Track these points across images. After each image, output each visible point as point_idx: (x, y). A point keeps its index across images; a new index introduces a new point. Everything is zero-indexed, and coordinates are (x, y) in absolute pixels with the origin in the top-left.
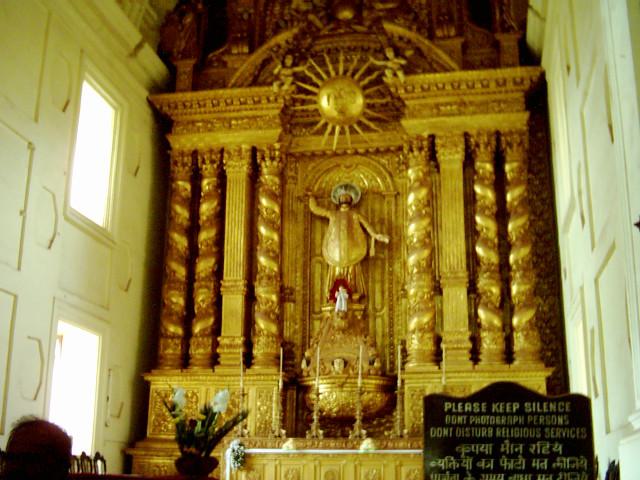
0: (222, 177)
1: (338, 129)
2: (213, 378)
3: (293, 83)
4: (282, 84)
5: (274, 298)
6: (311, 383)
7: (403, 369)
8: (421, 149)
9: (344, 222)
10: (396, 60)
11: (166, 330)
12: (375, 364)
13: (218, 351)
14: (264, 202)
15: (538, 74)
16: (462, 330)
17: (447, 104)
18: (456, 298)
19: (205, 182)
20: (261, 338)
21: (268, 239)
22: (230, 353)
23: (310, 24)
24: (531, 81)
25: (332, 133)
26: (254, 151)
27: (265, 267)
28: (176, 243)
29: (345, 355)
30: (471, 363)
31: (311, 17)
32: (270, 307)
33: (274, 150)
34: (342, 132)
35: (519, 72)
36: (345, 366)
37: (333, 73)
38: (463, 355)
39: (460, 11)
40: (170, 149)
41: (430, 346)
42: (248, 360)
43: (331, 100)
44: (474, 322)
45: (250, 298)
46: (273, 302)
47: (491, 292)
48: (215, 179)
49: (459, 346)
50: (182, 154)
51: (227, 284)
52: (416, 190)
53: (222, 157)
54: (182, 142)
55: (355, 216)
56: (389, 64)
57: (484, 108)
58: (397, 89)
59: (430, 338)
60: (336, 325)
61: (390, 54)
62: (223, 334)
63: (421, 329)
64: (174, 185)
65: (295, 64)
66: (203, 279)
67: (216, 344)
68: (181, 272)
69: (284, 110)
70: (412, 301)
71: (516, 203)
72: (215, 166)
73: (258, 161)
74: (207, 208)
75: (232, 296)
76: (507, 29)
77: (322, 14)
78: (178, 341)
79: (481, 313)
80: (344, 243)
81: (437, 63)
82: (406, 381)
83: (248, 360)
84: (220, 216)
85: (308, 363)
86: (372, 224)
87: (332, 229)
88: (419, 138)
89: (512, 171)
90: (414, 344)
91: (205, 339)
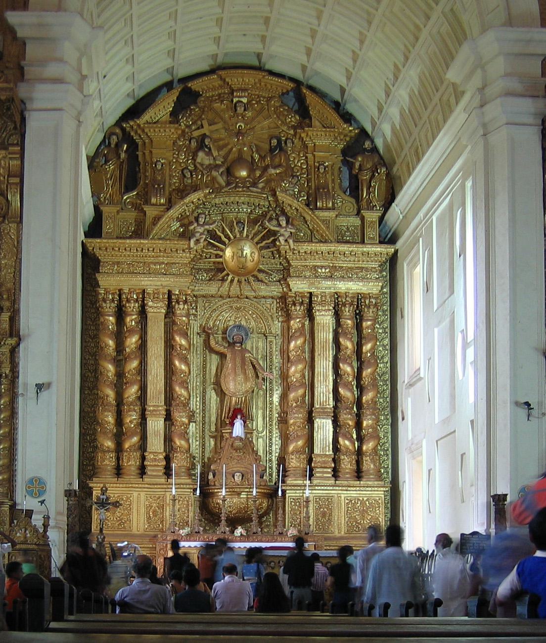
0: (143, 313)
1: (236, 279)
2: (143, 486)
3: (205, 240)
4: (198, 241)
5: (185, 420)
6: (216, 491)
7: (283, 482)
8: (302, 303)
9: (238, 360)
10: (288, 230)
11: (102, 445)
12: (264, 477)
13: (146, 463)
14: (177, 338)
15: (393, 250)
16: (327, 453)
17: (322, 267)
18: (324, 429)
19: (128, 319)
21: (182, 371)
22: (155, 466)
23: (214, 179)
24: (387, 254)
25: (232, 281)
26: (170, 292)
27: (181, 395)
28: (108, 371)
30: (334, 479)
31: (214, 173)
33: (186, 295)
34: (239, 282)
35: (379, 249)
36: (242, 479)
37: (238, 236)
38: (328, 473)
39: (333, 181)
40: (99, 286)
41: (303, 464)
42: (168, 471)
43: (235, 257)
44: (336, 448)
45: (168, 418)
47: (349, 425)
48: (136, 316)
49: (326, 466)
50: (107, 292)
51: (151, 408)
52: (297, 338)
53: (143, 298)
54: (107, 282)
55: (247, 355)
56: (282, 231)
57: (348, 274)
58: (286, 252)
59: (304, 459)
61: (284, 223)
62: (148, 450)
63: (297, 451)
64: (102, 320)
65: (205, 224)
66: (131, 403)
67: (143, 458)
68: (110, 393)
69: (193, 260)
71: (369, 355)
72: (137, 305)
73: (174, 303)
74: (132, 341)
75: (154, 419)
76: (371, 208)
77: (221, 170)
78: (113, 455)
79: (340, 440)
80: (240, 378)
81: (317, 231)
82: (287, 492)
83: (168, 471)
84: (143, 347)
85: (214, 477)
87: (229, 364)
88: (302, 295)
89: (368, 328)
90: (295, 462)
91: (135, 454)
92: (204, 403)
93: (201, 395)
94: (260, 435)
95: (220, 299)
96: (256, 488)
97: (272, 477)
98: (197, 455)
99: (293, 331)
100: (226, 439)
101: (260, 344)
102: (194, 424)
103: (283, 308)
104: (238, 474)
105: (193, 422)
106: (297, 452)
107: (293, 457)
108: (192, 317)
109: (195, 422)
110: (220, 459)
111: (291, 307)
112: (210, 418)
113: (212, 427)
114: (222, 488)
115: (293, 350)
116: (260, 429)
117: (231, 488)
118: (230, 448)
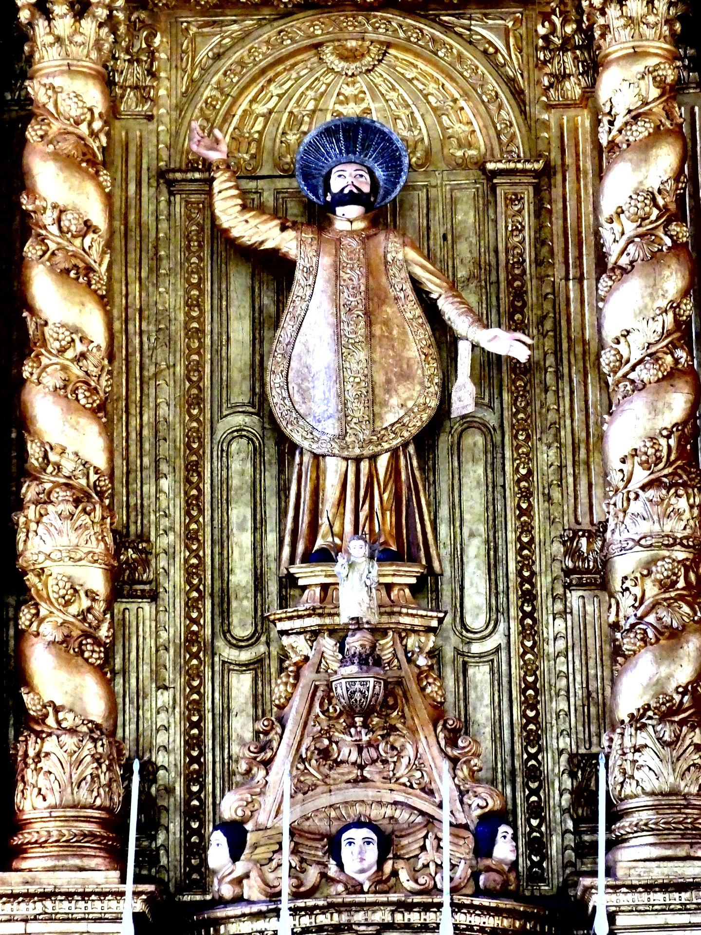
20: (50, 745)
29: (376, 813)
32: (83, 616)
36: (381, 861)
46: (91, 594)
60: (340, 689)
70: (626, 601)
86: (453, 286)
92: (192, 504)
93: (180, 463)
94: (476, 648)
95: (266, 12)
96: (457, 907)
97: (545, 857)
98: (161, 759)
99: (618, 124)
100: (299, 667)
101: (466, 216)
102: (147, 609)
103: (566, 39)
104: (358, 834)
105: (143, 595)
106: (664, 717)
107: (642, 738)
108: (130, 102)
109: (153, 597)
110: (267, 764)
111: (603, 13)
112: (223, 571)
113: (235, 619)
114: (277, 912)
115: (620, 212)
116: (476, 620)
117: (324, 910)
118: (317, 709)
